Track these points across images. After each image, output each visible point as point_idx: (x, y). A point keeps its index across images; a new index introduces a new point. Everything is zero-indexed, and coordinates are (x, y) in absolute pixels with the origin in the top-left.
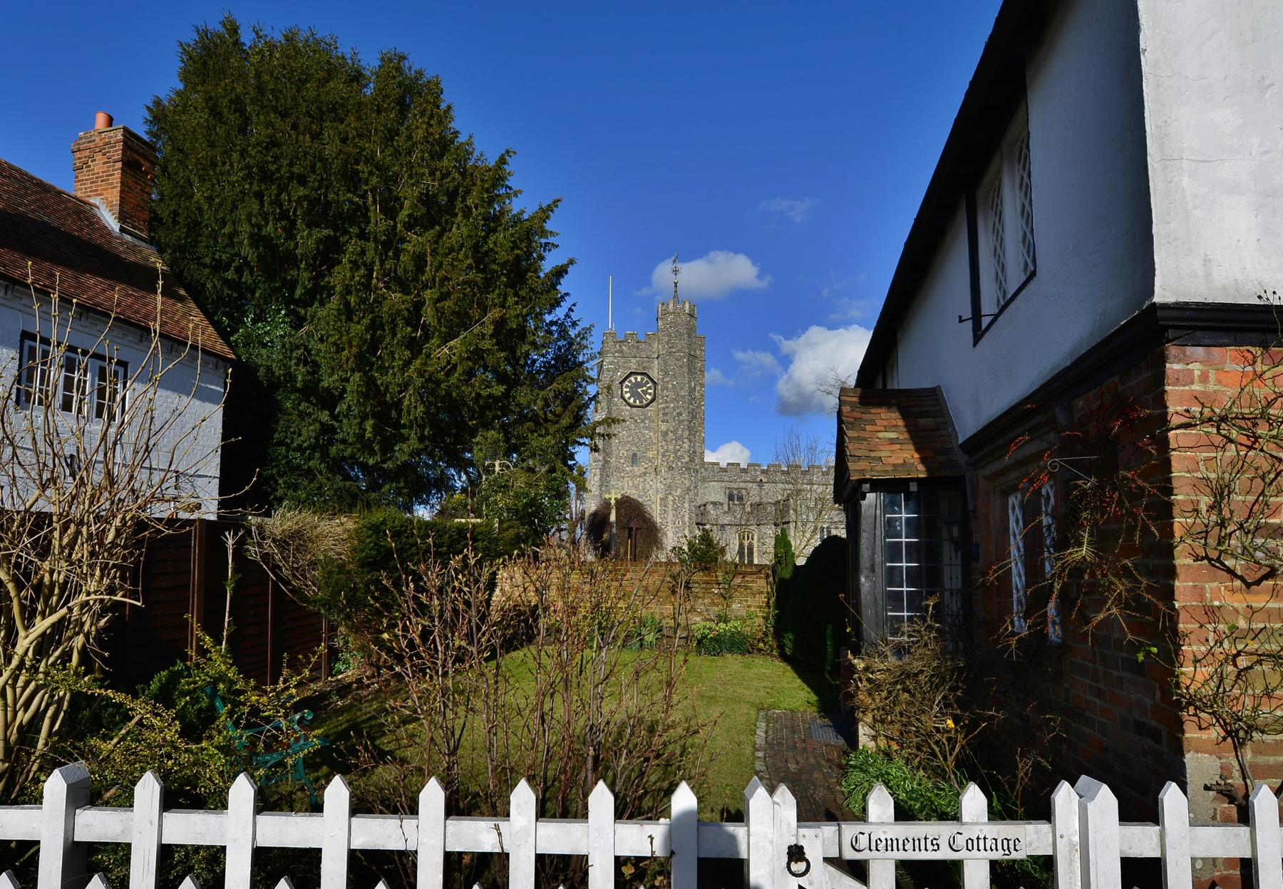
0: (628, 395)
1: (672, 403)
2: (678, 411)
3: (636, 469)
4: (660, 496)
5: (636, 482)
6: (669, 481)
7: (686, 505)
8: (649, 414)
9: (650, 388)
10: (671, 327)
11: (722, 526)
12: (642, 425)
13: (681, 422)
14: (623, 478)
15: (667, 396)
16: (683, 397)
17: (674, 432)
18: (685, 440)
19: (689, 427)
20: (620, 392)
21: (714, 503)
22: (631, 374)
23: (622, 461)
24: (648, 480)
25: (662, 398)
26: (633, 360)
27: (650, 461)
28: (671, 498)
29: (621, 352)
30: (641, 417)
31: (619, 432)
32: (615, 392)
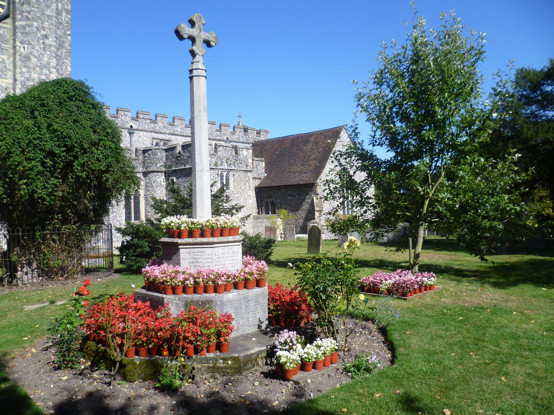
1: (36, 21)
2: (43, 32)
15: (29, 12)
17: (39, 58)
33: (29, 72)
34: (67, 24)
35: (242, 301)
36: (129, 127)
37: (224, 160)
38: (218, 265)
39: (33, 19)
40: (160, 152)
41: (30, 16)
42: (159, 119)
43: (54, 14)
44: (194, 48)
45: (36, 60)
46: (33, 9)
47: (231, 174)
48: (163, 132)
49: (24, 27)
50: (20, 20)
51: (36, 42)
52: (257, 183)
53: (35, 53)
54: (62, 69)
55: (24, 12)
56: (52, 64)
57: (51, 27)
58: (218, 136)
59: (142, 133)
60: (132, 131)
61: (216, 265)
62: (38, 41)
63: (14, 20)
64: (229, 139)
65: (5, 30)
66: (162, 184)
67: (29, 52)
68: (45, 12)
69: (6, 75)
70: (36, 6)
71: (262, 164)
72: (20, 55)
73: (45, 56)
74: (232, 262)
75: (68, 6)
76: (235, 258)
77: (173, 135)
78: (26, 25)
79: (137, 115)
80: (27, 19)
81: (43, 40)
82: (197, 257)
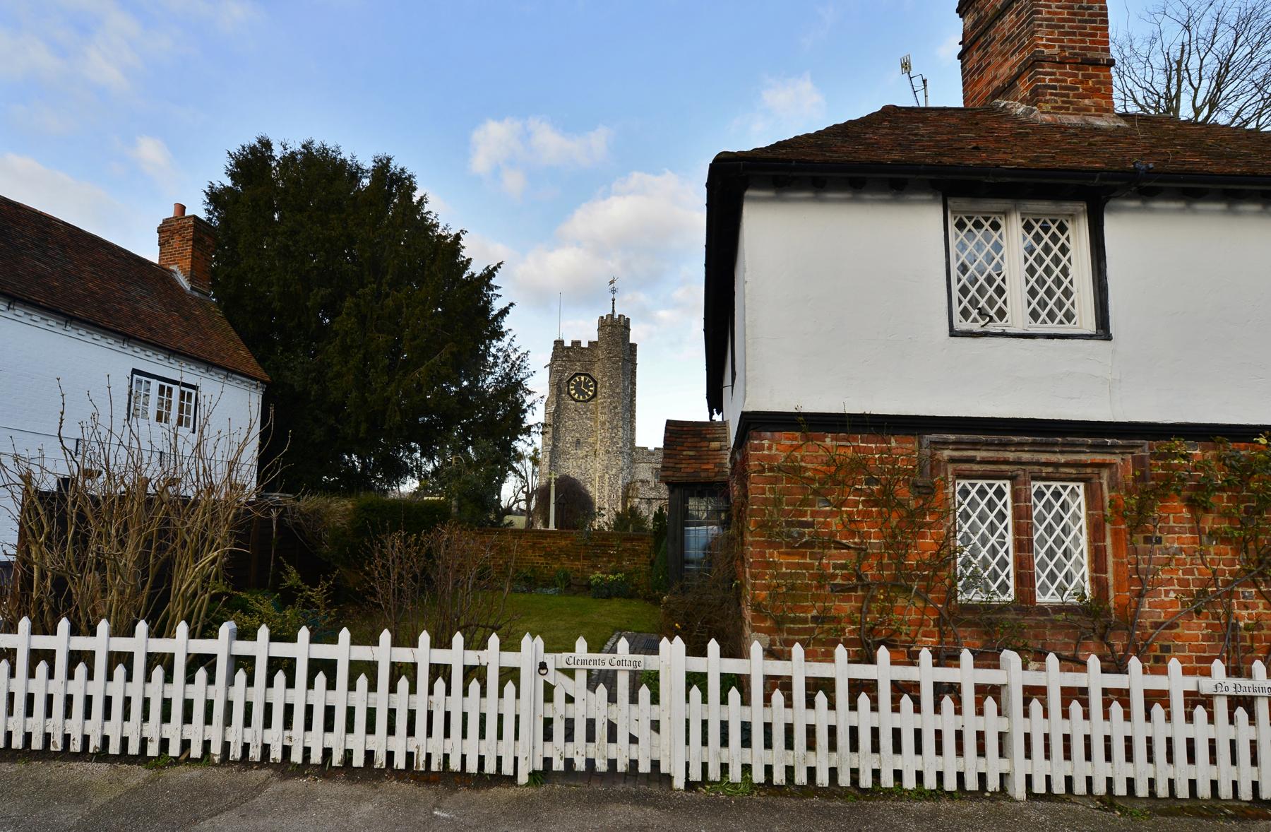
0: (573, 392)
3: (579, 452)
4: (598, 474)
5: (579, 463)
6: (606, 462)
7: (620, 482)
11: (649, 499)
13: (616, 414)
14: (569, 459)
16: (618, 394)
17: (610, 422)
18: (620, 429)
19: (623, 418)
21: (642, 481)
22: (576, 375)
23: (568, 445)
24: (589, 461)
27: (591, 446)
28: (607, 476)
29: (568, 356)
80: (605, 397)
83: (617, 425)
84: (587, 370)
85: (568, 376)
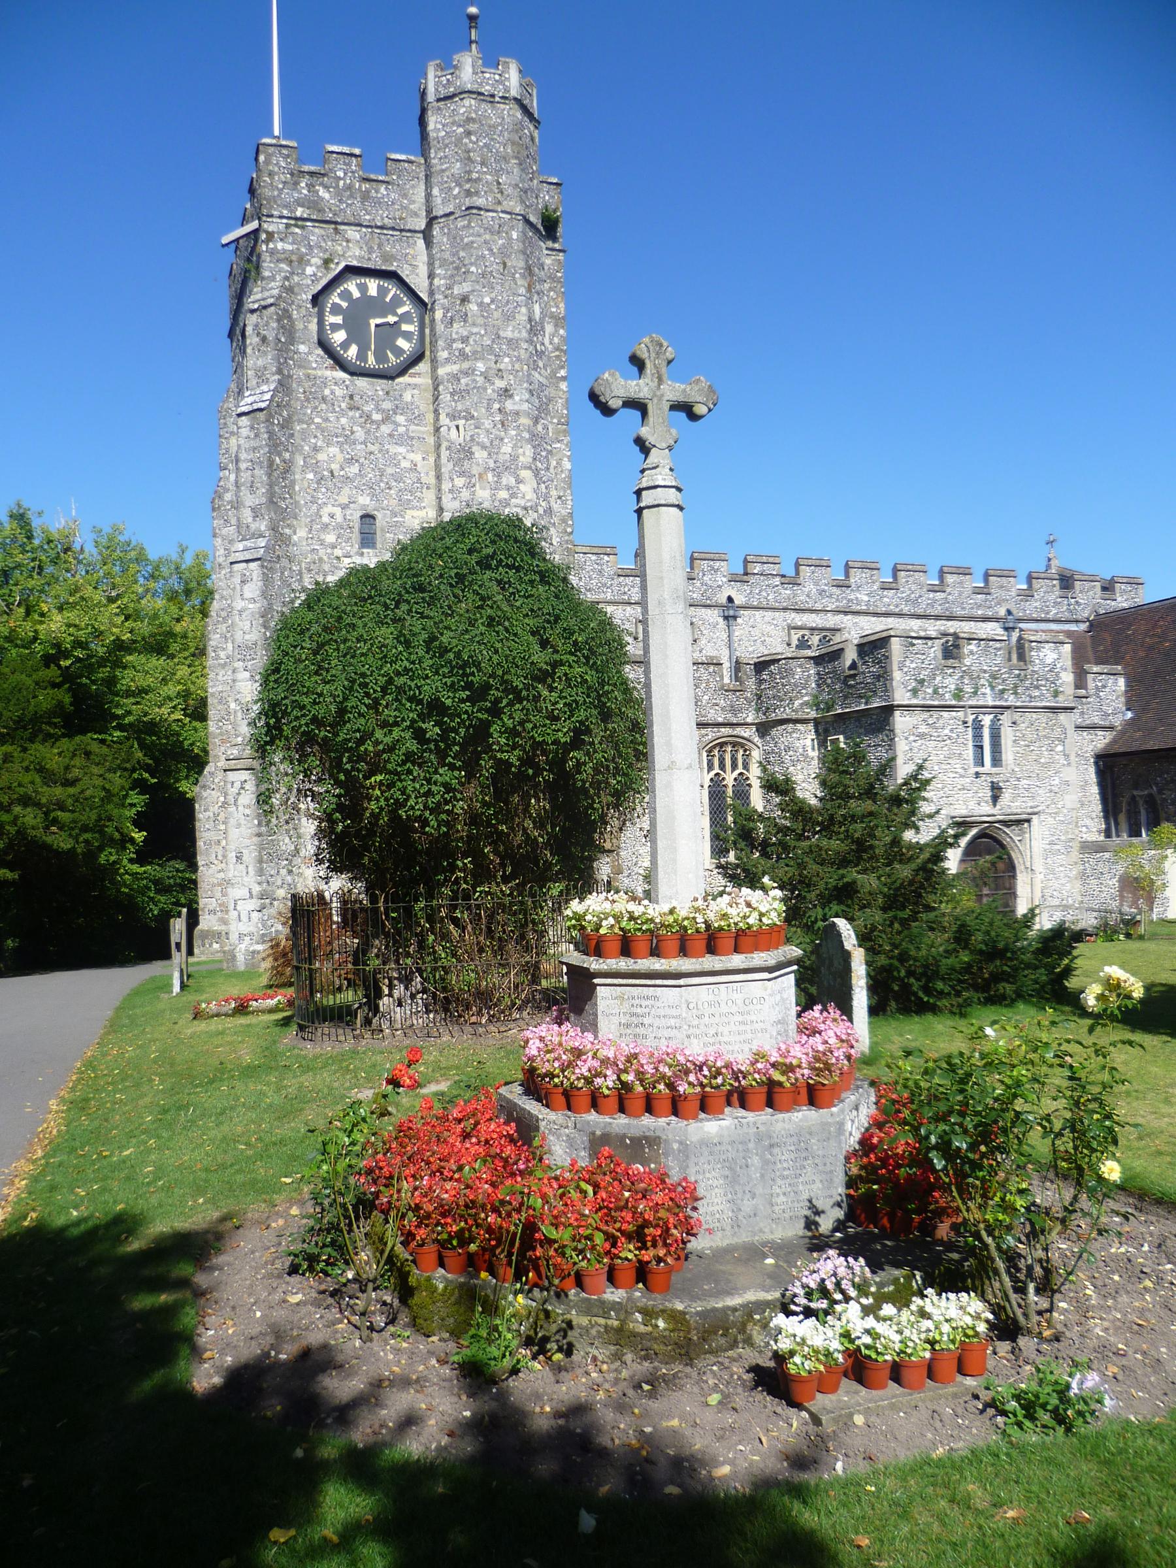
2: (500, 384)
8: (407, 397)
9: (405, 318)
10: (468, 133)
12: (386, 429)
15: (465, 340)
19: (534, 436)
20: (313, 327)
23: (330, 538)
25: (449, 346)
26: (352, 233)
29: (314, 204)
30: (387, 405)
31: (316, 449)
32: (299, 325)
33: (470, 486)
34: (557, 353)
35: (751, 1145)
36: (724, 600)
37: (982, 681)
38: (696, 1037)
39: (476, 356)
40: (800, 666)
41: (468, 349)
42: (806, 571)
43: (524, 334)
44: (644, 432)
45: (485, 454)
46: (475, 330)
47: (1006, 718)
48: (819, 606)
49: (456, 378)
50: (447, 360)
51: (483, 410)
52: (1101, 741)
53: (483, 438)
54: (548, 469)
55: (454, 341)
56: (521, 458)
57: (517, 366)
58: (979, 607)
59: (758, 614)
60: (731, 613)
61: (688, 1037)
62: (489, 408)
63: (434, 362)
64: (1014, 612)
65: (416, 392)
66: (807, 756)
67: (468, 438)
68: (502, 333)
69: (420, 499)
70: (480, 321)
71: (1116, 682)
72: (448, 448)
73: (506, 440)
74: (742, 1028)
75: (557, 307)
76: (754, 1018)
77: (846, 613)
78: (461, 371)
79: (745, 567)
80: (463, 356)
81: (500, 402)
82: (639, 1010)
83: (514, 458)
84: (387, 258)
85: (315, 278)
